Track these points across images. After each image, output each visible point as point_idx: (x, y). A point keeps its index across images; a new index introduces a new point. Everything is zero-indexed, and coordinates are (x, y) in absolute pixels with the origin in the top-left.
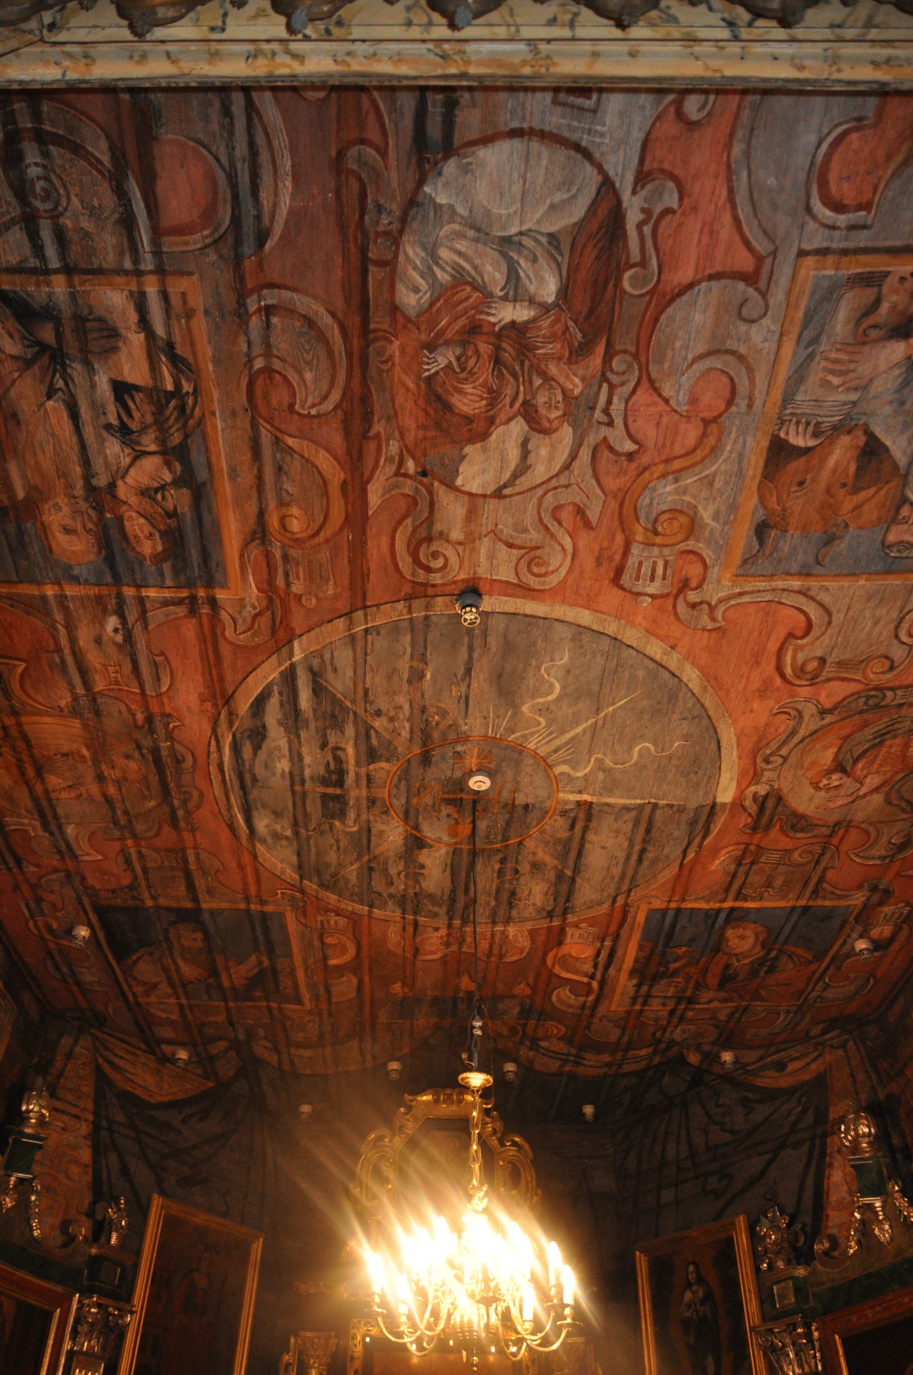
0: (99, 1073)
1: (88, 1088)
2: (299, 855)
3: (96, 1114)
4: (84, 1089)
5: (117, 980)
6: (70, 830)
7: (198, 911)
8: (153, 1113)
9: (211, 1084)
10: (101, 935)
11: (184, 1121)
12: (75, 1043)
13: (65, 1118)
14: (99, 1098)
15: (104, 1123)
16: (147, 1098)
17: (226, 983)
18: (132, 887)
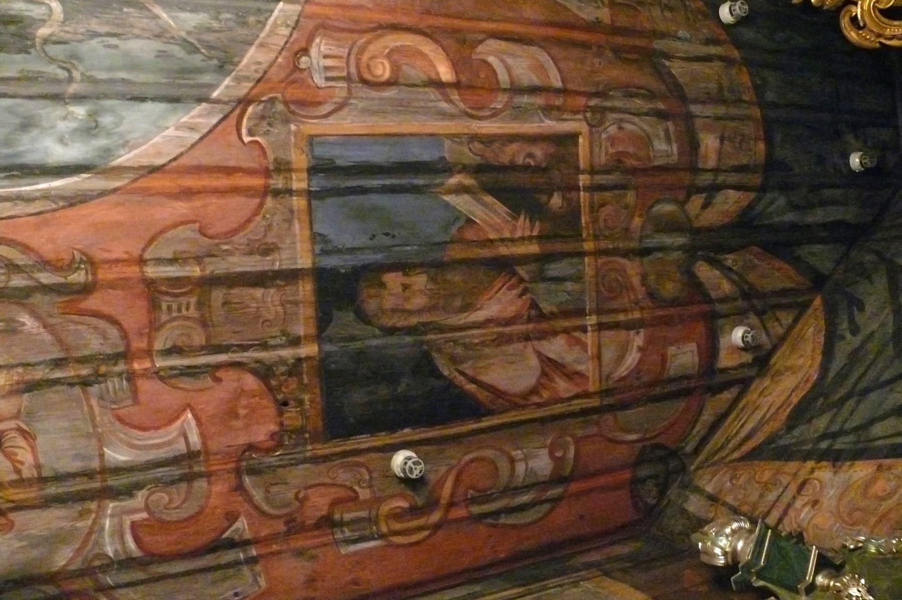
0: (754, 455)
1: (766, 471)
2: (142, 99)
3: (807, 456)
4: (767, 475)
5: (542, 421)
6: (118, 456)
7: (320, 275)
8: (831, 374)
9: (818, 302)
10: (407, 433)
11: (855, 331)
12: (699, 490)
13: (798, 504)
14: (785, 454)
15: (824, 445)
16: (809, 385)
17: (534, 248)
18: (264, 372)
